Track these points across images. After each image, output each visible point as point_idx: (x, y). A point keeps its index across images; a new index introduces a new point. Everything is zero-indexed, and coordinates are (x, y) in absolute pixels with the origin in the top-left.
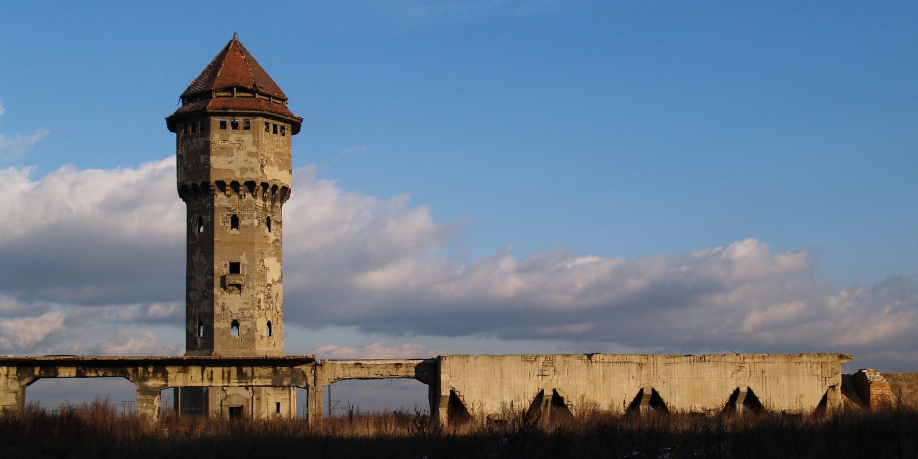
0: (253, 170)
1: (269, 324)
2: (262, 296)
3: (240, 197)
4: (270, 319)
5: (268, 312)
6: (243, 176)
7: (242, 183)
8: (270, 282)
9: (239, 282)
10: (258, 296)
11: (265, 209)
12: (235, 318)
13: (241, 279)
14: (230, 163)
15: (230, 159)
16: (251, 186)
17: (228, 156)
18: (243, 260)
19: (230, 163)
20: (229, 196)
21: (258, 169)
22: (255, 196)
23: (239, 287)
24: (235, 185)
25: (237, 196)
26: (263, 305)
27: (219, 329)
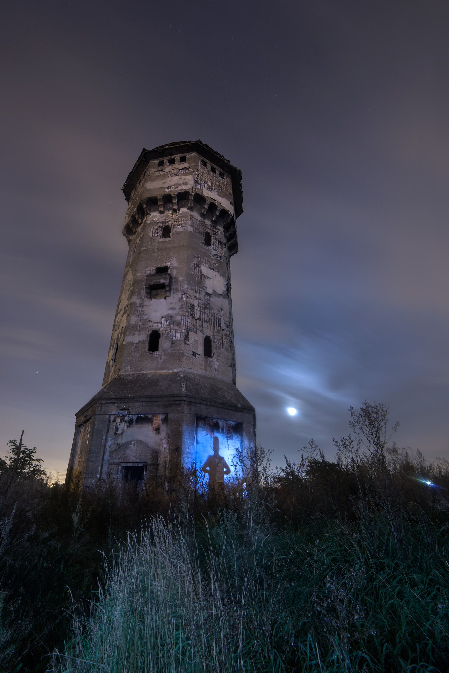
0: (186, 184)
1: (207, 342)
2: (196, 303)
3: (175, 211)
4: (208, 333)
5: (205, 325)
6: (176, 189)
7: (173, 194)
8: (210, 291)
9: (162, 281)
10: (191, 301)
11: (202, 224)
12: (155, 327)
13: (165, 278)
14: (164, 183)
15: (164, 181)
16: (183, 196)
17: (162, 180)
18: (173, 263)
19: (164, 183)
20: (162, 212)
21: (192, 182)
22: (190, 208)
23: (162, 286)
24: (168, 199)
25: (171, 212)
26: (197, 314)
27: (131, 343)
